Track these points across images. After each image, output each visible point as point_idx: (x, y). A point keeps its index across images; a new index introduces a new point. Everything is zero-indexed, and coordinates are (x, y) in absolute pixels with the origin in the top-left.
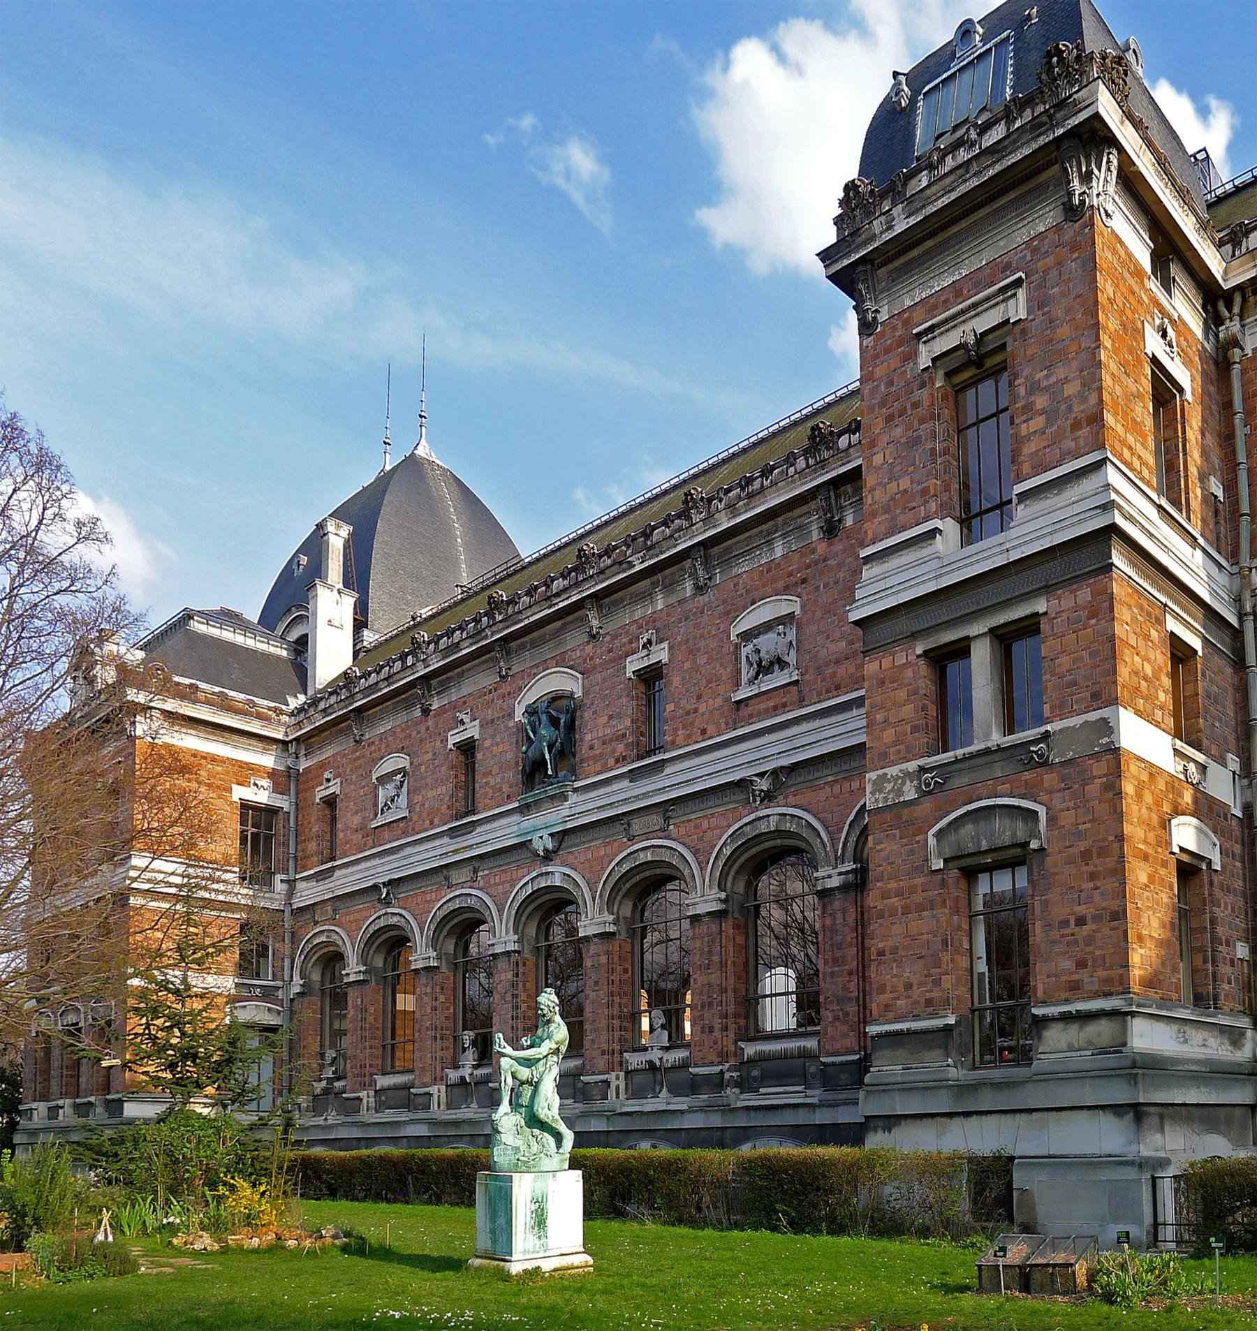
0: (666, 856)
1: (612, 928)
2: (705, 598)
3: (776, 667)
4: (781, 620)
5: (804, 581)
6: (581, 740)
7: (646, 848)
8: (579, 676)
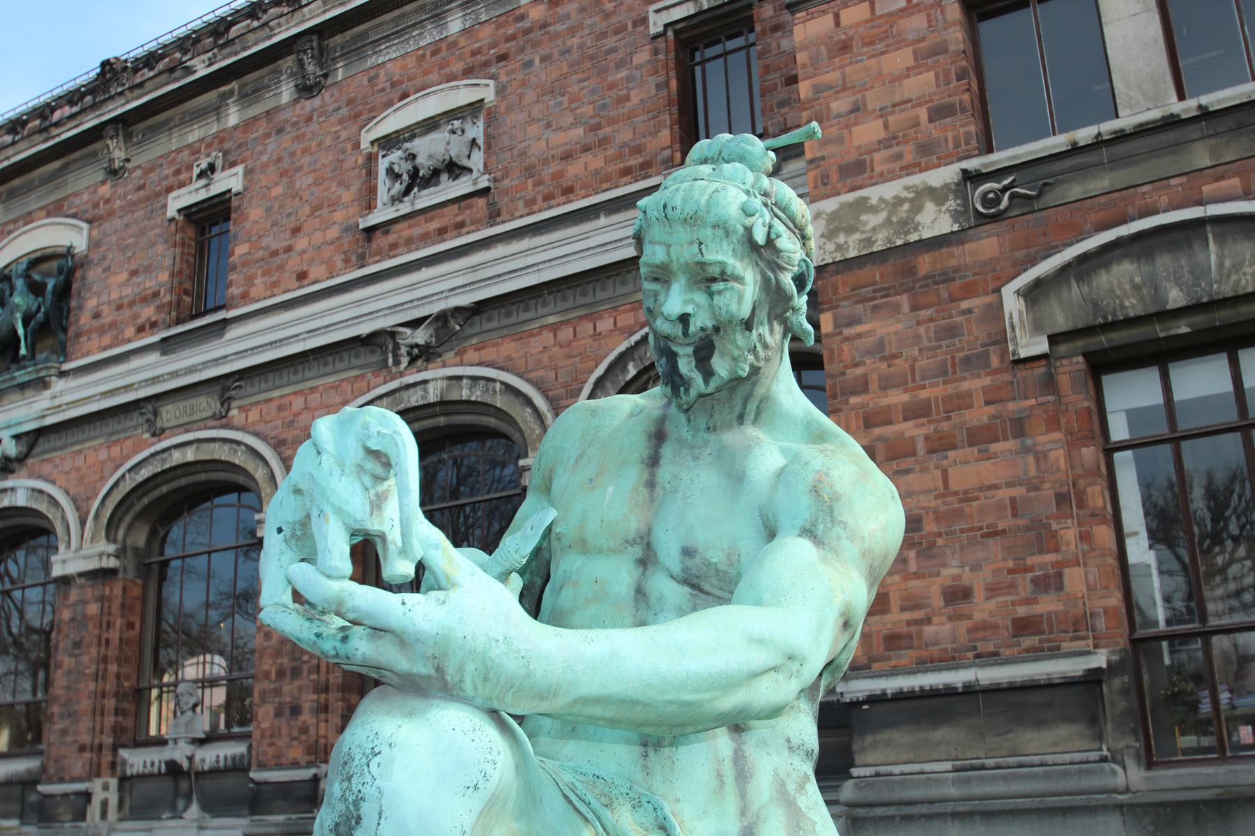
0: (222, 453)
1: (112, 563)
2: (317, 102)
3: (444, 177)
4: (451, 115)
5: (502, 58)
6: (80, 308)
7: (183, 443)
8: (85, 226)
